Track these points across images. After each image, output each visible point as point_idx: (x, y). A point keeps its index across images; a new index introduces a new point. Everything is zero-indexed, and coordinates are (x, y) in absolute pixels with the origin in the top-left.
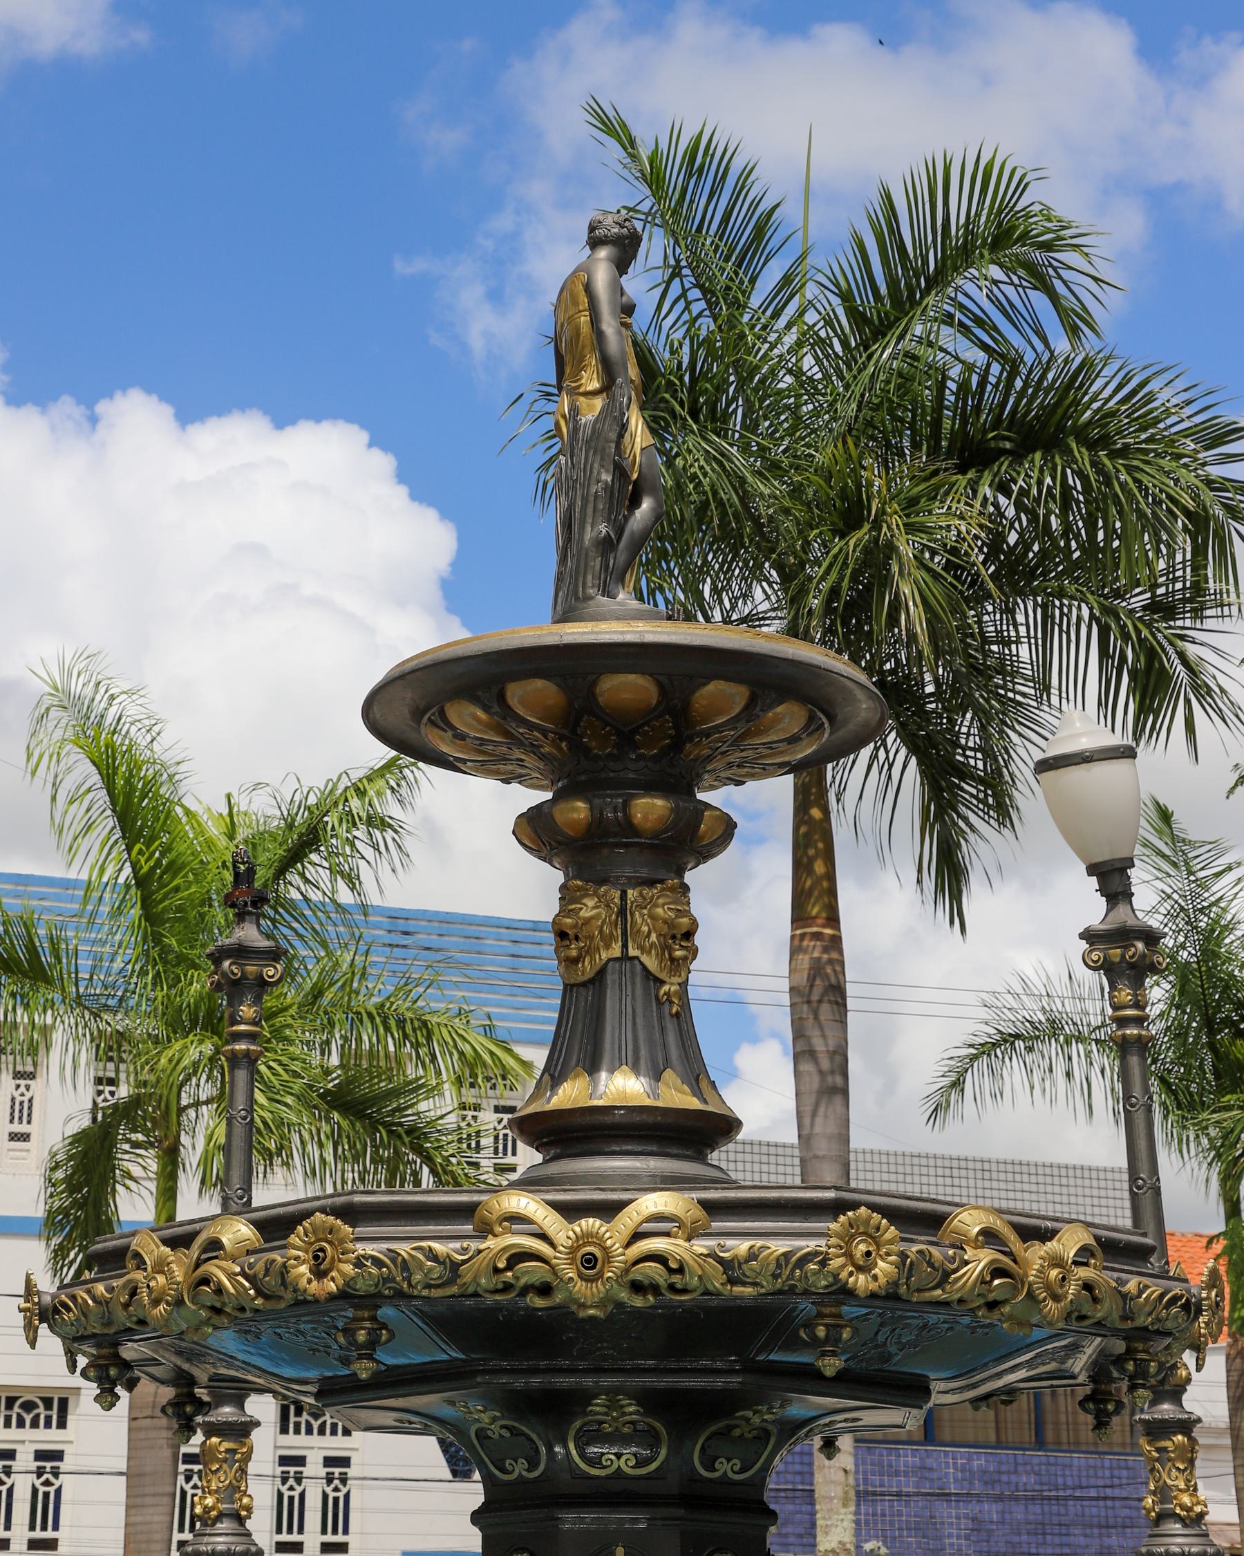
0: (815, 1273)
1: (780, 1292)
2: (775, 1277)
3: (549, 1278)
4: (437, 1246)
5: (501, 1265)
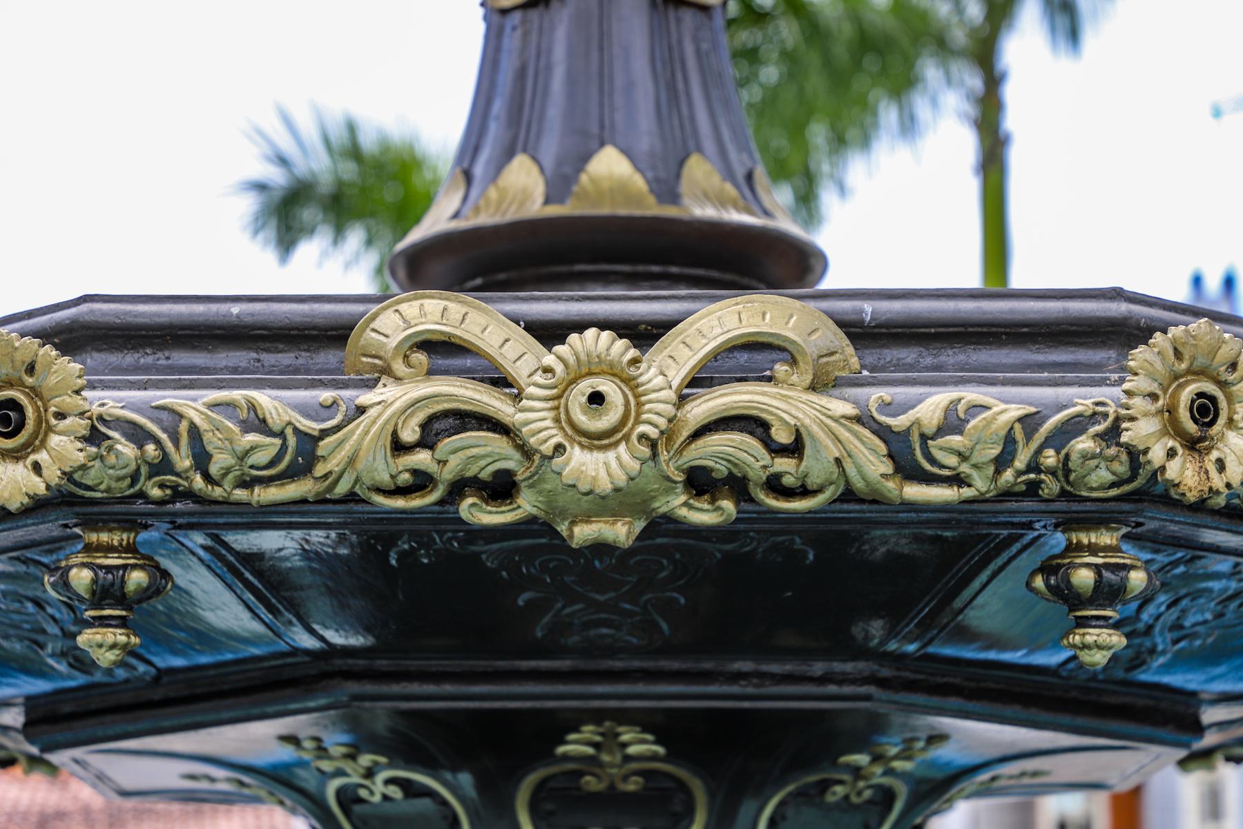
0: (1086, 456)
1: (1007, 495)
2: (1002, 462)
3: (512, 461)
4: (265, 399)
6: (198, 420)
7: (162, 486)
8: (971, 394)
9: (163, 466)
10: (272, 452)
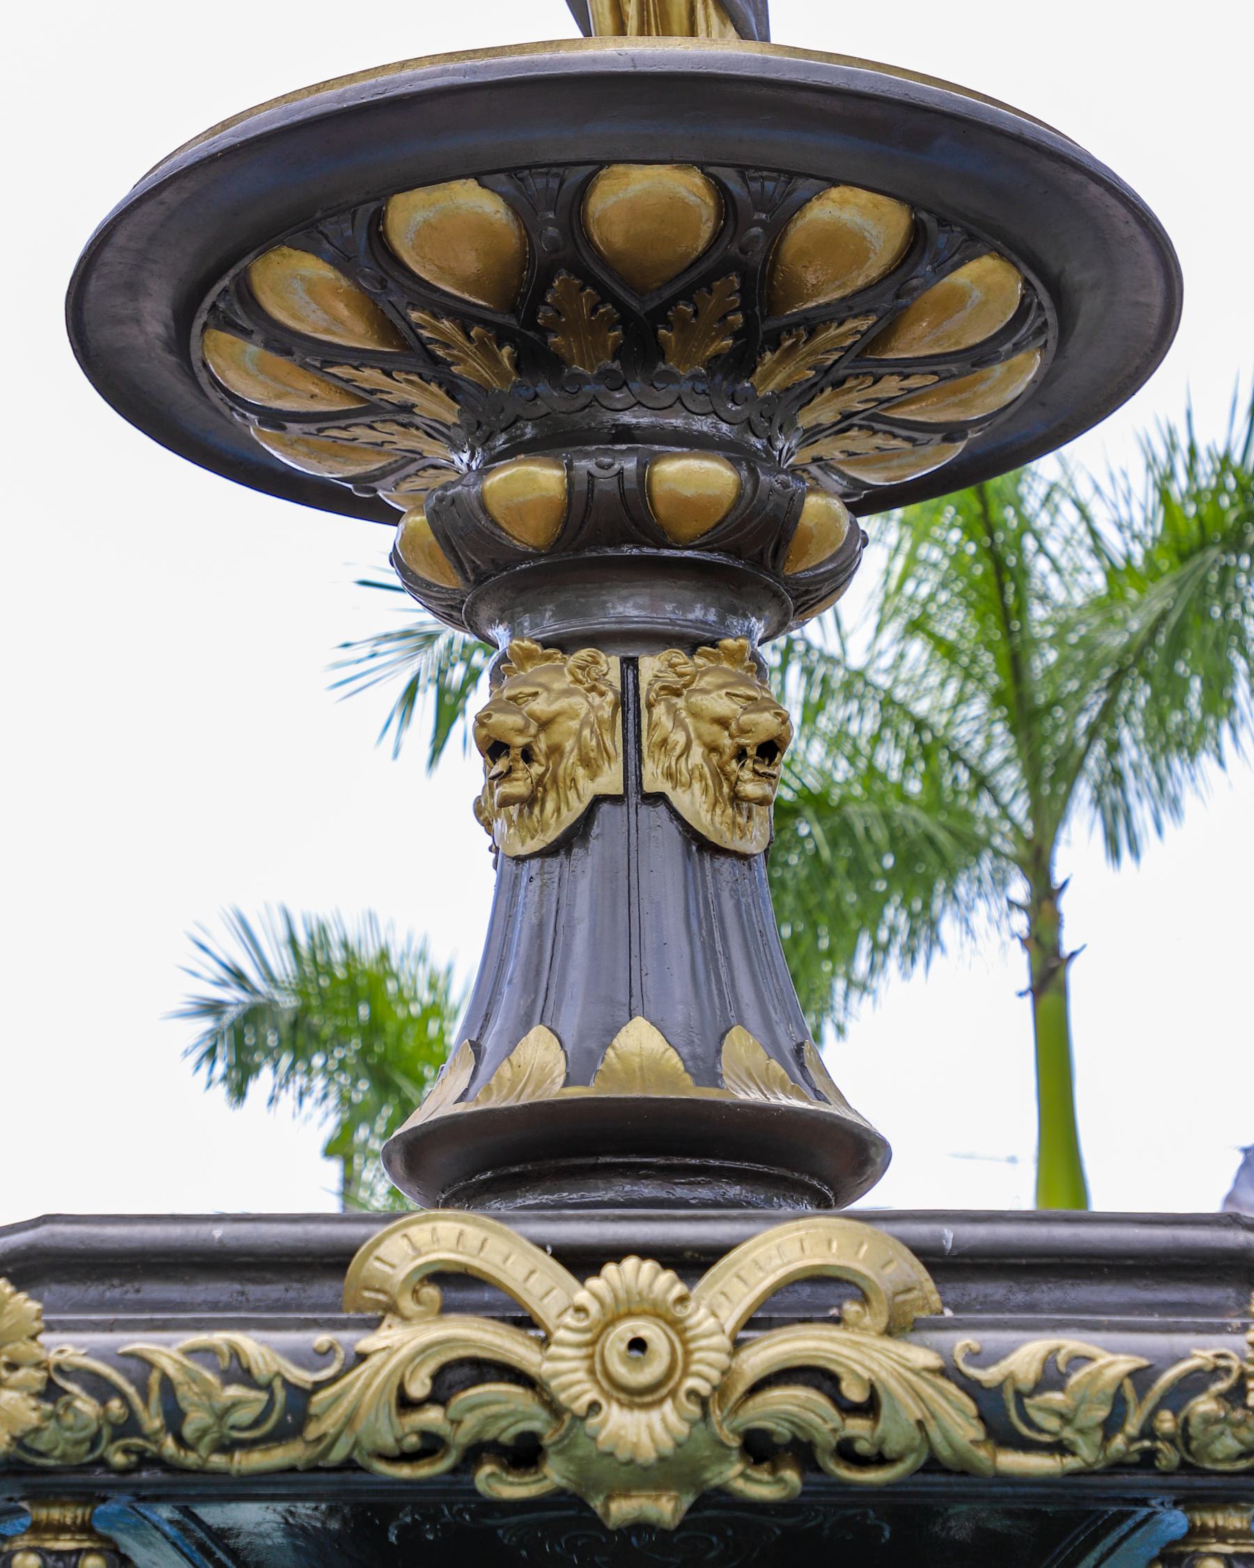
0: (1209, 1420)
1: (1118, 1466)
2: (1111, 1426)
3: (538, 1422)
4: (252, 1344)
5: (419, 1388)
6: (171, 1370)
7: (126, 1451)
8: (1071, 1343)
9: (130, 1426)
10: (256, 1409)
